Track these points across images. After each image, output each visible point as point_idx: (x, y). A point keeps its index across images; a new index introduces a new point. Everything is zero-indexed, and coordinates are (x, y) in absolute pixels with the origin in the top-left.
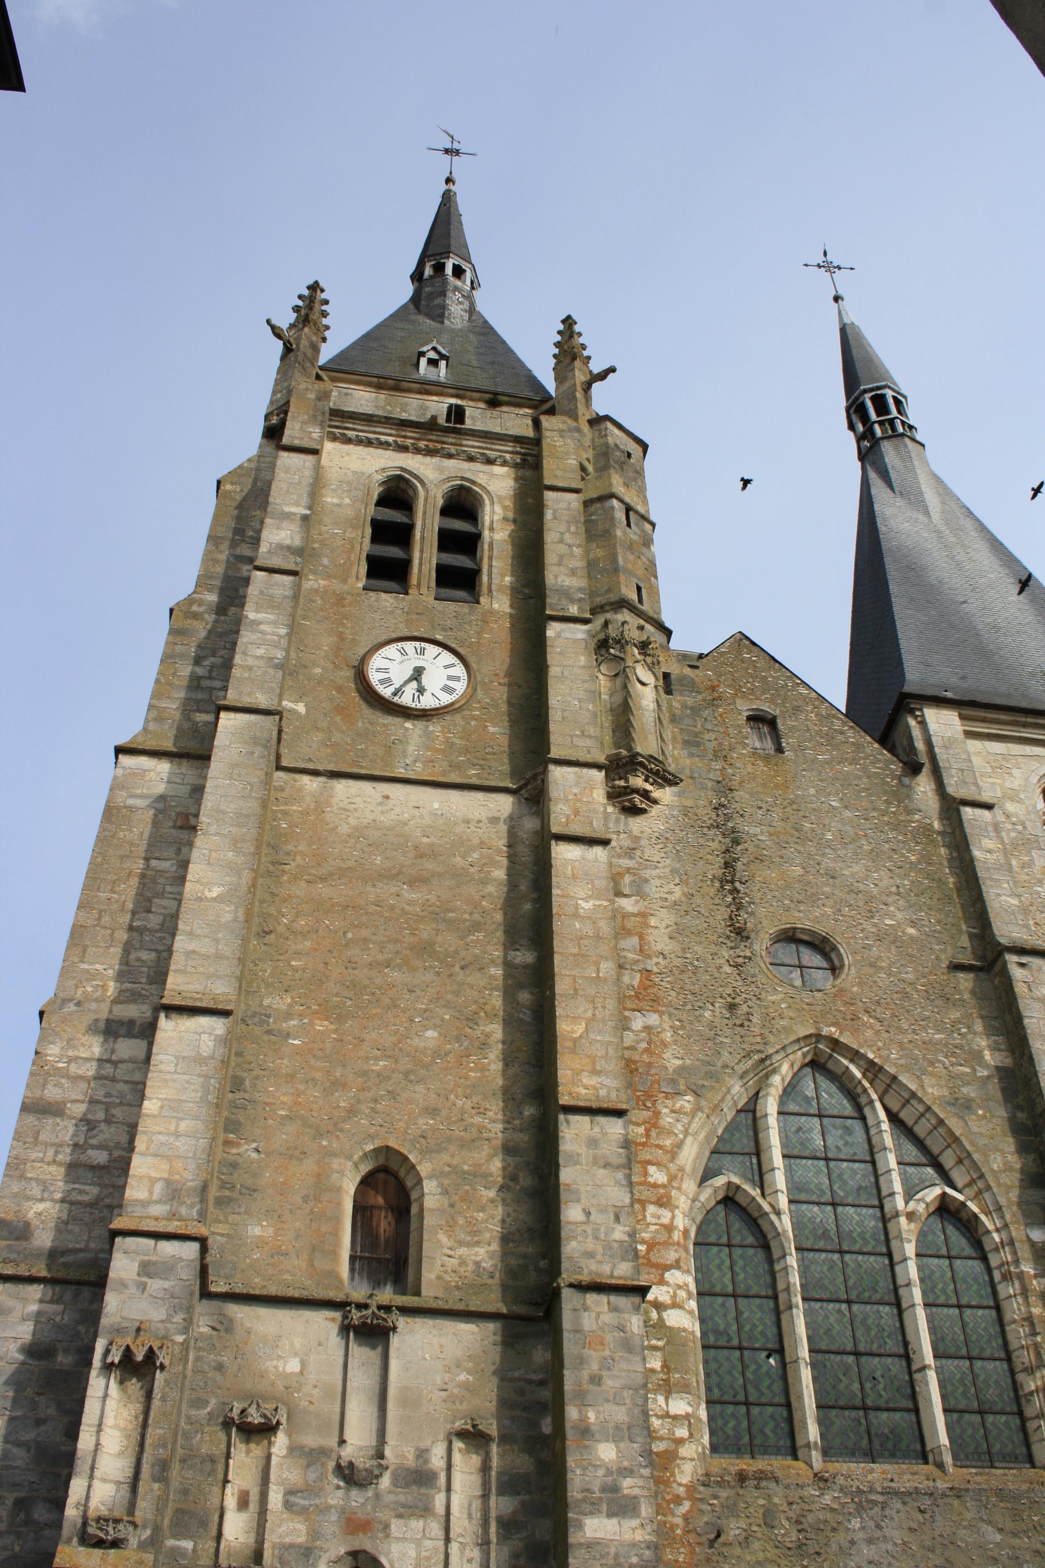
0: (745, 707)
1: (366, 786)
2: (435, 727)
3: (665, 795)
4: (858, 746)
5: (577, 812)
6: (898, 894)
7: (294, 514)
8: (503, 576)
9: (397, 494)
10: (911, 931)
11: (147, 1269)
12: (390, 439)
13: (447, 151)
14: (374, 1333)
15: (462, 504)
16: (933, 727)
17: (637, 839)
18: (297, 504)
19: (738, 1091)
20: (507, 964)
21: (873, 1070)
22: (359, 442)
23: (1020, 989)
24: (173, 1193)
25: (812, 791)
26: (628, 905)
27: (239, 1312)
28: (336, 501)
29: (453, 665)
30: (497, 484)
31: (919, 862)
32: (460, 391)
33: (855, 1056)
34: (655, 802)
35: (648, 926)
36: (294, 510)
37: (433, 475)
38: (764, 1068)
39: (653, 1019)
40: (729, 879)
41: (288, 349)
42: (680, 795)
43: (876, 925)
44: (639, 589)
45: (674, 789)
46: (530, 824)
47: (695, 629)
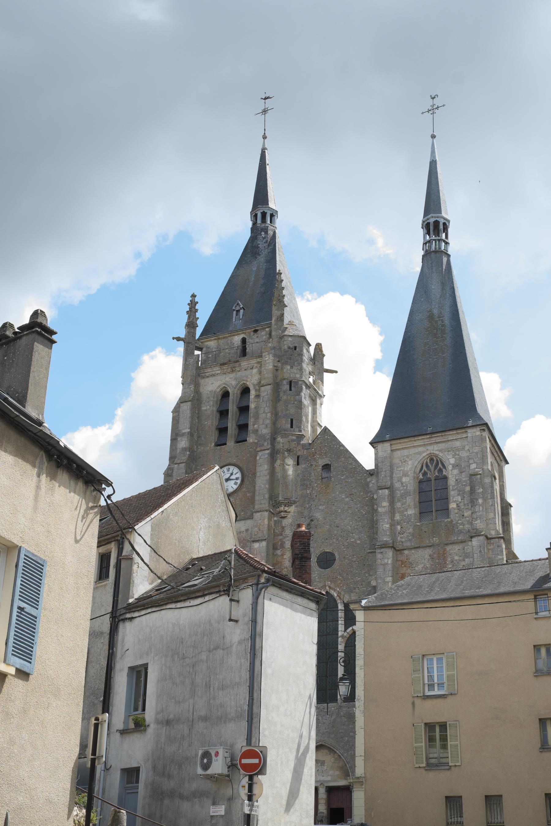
0: (322, 462)
3: (292, 509)
5: (260, 530)
6: (357, 529)
7: (185, 433)
8: (254, 425)
10: (358, 542)
12: (219, 372)
13: (268, 98)
15: (246, 391)
17: (283, 528)
18: (186, 428)
25: (337, 493)
28: (205, 408)
29: (237, 473)
31: (366, 514)
34: (289, 512)
35: (283, 559)
36: (184, 431)
42: (297, 507)
43: (348, 542)
44: (292, 420)
45: (296, 505)
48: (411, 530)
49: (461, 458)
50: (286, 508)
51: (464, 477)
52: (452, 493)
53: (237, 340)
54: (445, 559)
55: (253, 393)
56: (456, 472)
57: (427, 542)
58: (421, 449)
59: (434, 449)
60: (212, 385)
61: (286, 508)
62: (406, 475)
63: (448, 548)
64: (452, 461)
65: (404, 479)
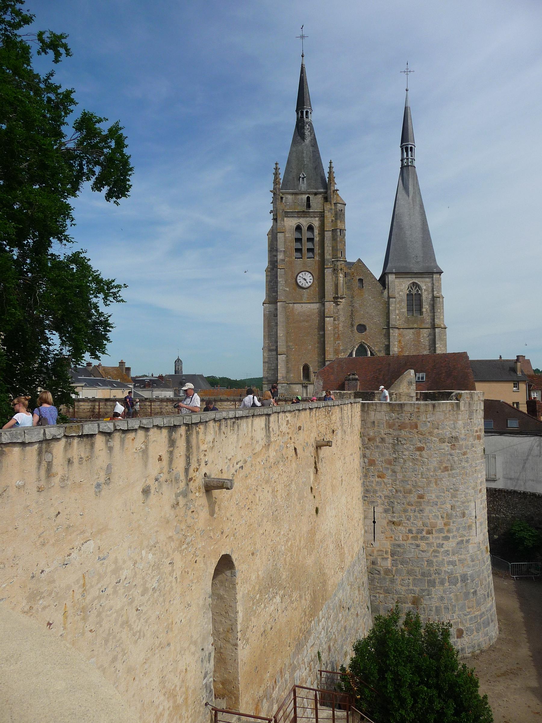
1: (299, 304)
2: (308, 290)
3: (343, 300)
4: (376, 284)
9: (298, 228)
11: (282, 387)
14: (306, 387)
16: (390, 279)
19: (350, 351)
20: (319, 334)
21: (368, 346)
22: (290, 217)
23: (391, 334)
24: (283, 378)
26: (336, 322)
27: (291, 385)
30: (316, 222)
32: (309, 194)
33: (366, 344)
37: (304, 222)
38: (354, 347)
39: (339, 342)
40: (352, 316)
41: (274, 194)
46: (323, 309)
47: (351, 258)
48: (404, 319)
49: (428, 286)
50: (341, 300)
51: (430, 296)
52: (424, 304)
53: (305, 197)
54: (420, 335)
55: (316, 232)
56: (426, 293)
57: (411, 326)
58: (409, 279)
59: (416, 281)
60: (291, 223)
61: (341, 300)
62: (402, 291)
63: (421, 330)
64: (424, 287)
65: (401, 293)
